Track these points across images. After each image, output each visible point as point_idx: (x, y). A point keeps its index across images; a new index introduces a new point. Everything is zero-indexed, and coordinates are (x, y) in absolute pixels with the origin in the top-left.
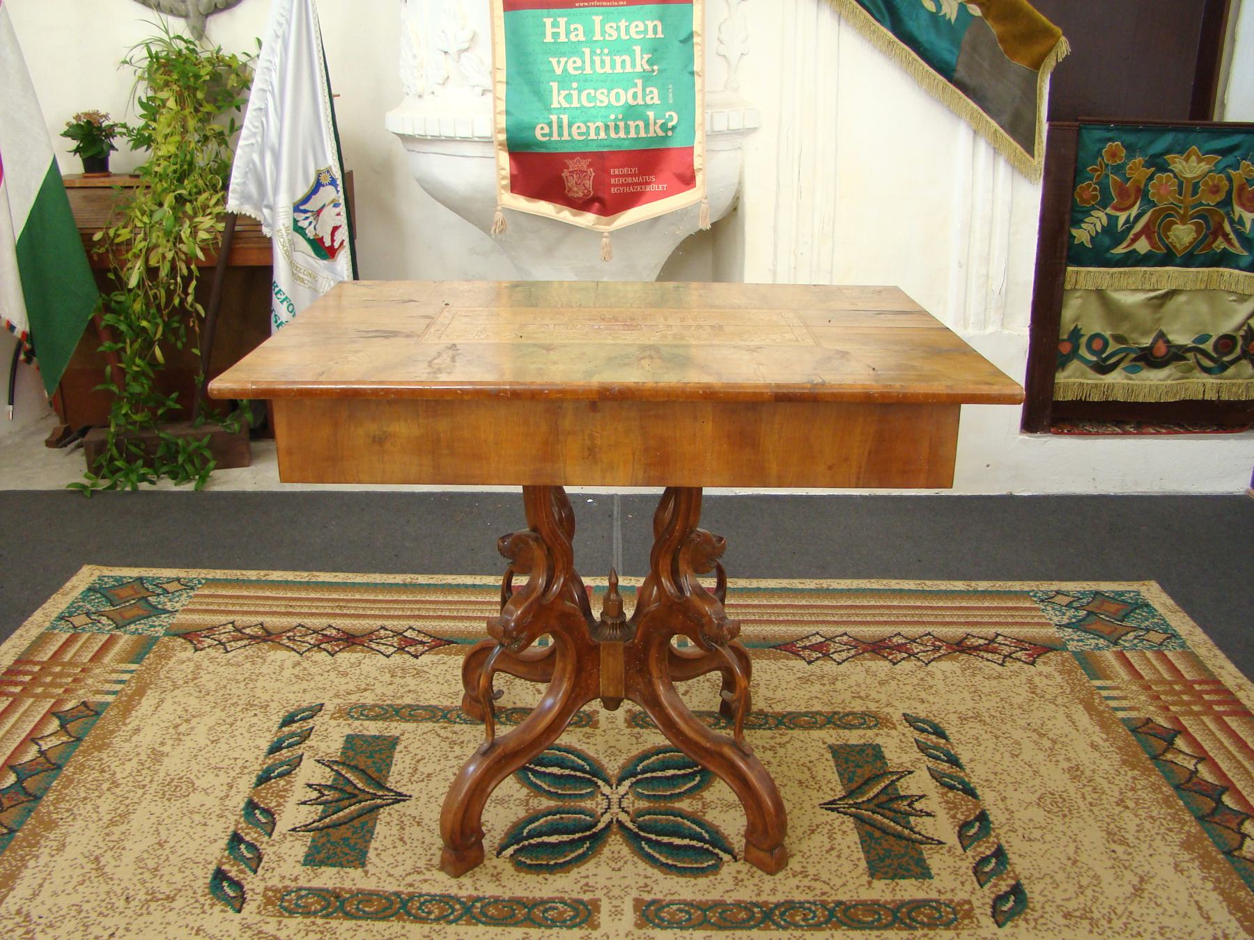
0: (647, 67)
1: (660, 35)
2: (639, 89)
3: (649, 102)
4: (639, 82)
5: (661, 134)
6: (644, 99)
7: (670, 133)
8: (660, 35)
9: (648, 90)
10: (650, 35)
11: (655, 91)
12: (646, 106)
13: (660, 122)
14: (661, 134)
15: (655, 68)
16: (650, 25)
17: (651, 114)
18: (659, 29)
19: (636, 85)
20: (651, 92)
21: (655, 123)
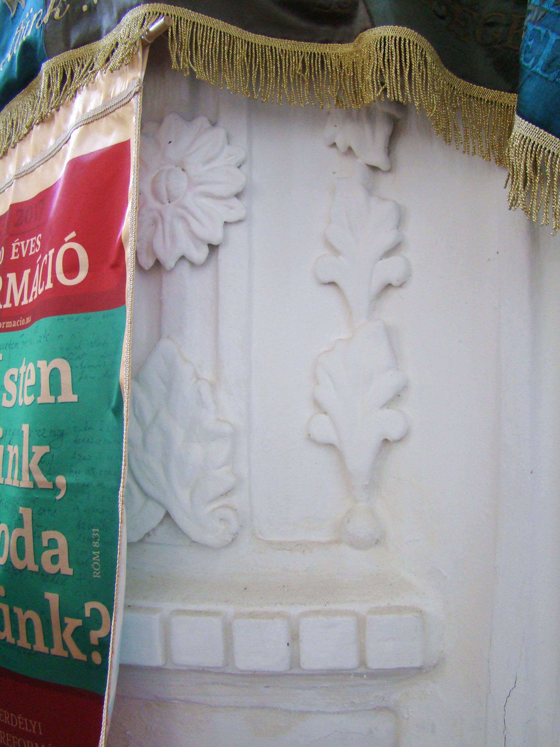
0: (40, 478)
1: (68, 396)
2: (27, 532)
3: (50, 568)
4: (27, 514)
5: (77, 654)
6: (37, 559)
7: (96, 658)
8: (68, 396)
9: (47, 535)
10: (46, 397)
11: (62, 541)
12: (42, 574)
13: (73, 623)
14: (77, 654)
15: (61, 480)
16: (45, 368)
17: (53, 598)
18: (66, 379)
19: (20, 523)
20: (53, 543)
21: (63, 626)
